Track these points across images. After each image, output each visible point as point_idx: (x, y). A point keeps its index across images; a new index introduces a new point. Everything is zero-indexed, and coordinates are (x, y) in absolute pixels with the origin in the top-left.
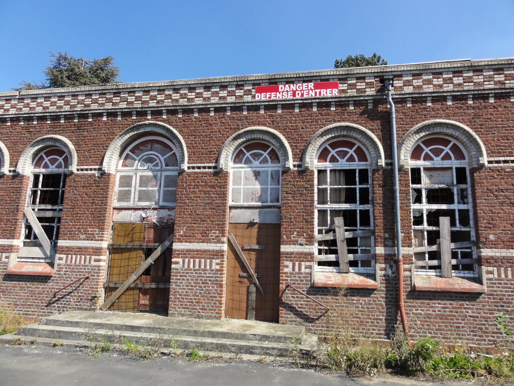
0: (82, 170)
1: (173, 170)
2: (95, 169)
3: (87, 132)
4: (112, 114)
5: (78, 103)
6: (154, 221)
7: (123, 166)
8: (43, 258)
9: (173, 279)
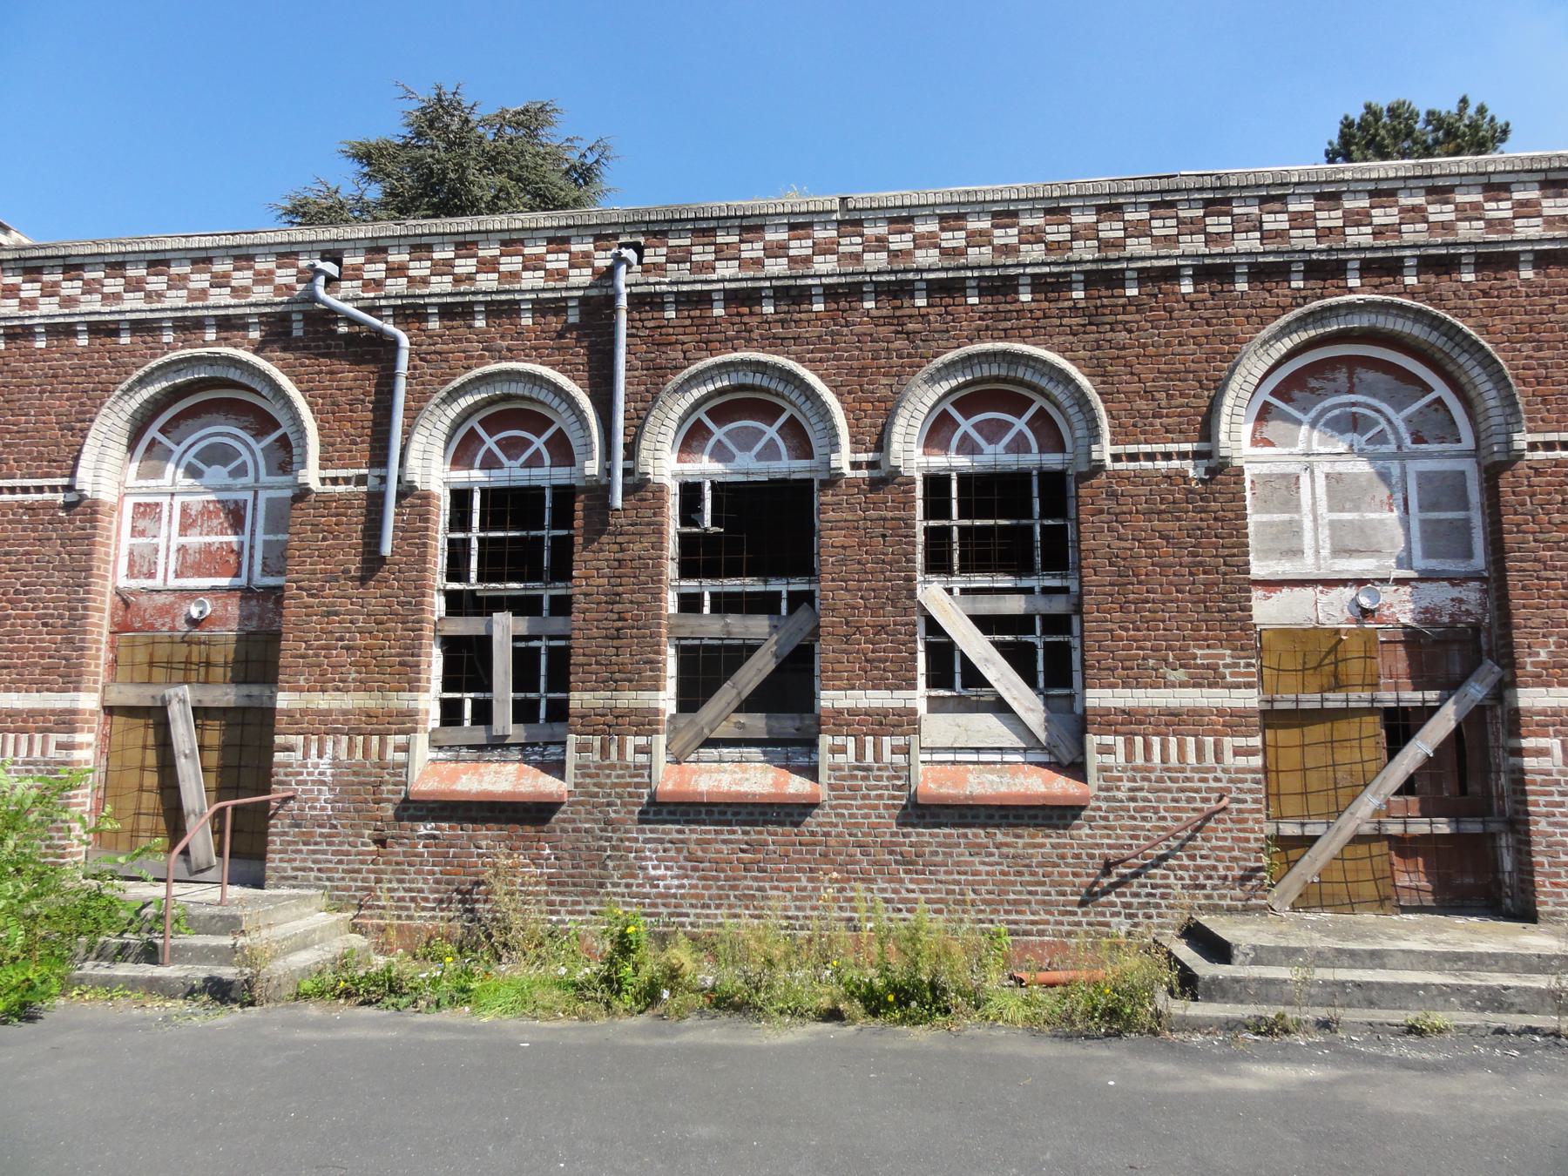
0: (1133, 457)
1: (1442, 455)
2: (1183, 456)
3: (1130, 332)
4: (1213, 273)
5: (1075, 235)
6: (1406, 619)
7: (1255, 442)
8: (1015, 750)
9: (1538, 804)
